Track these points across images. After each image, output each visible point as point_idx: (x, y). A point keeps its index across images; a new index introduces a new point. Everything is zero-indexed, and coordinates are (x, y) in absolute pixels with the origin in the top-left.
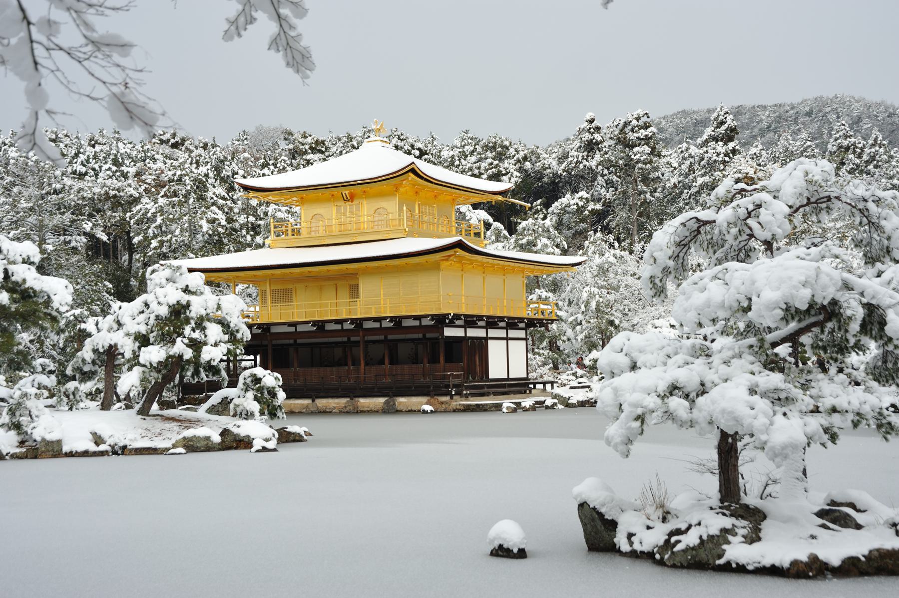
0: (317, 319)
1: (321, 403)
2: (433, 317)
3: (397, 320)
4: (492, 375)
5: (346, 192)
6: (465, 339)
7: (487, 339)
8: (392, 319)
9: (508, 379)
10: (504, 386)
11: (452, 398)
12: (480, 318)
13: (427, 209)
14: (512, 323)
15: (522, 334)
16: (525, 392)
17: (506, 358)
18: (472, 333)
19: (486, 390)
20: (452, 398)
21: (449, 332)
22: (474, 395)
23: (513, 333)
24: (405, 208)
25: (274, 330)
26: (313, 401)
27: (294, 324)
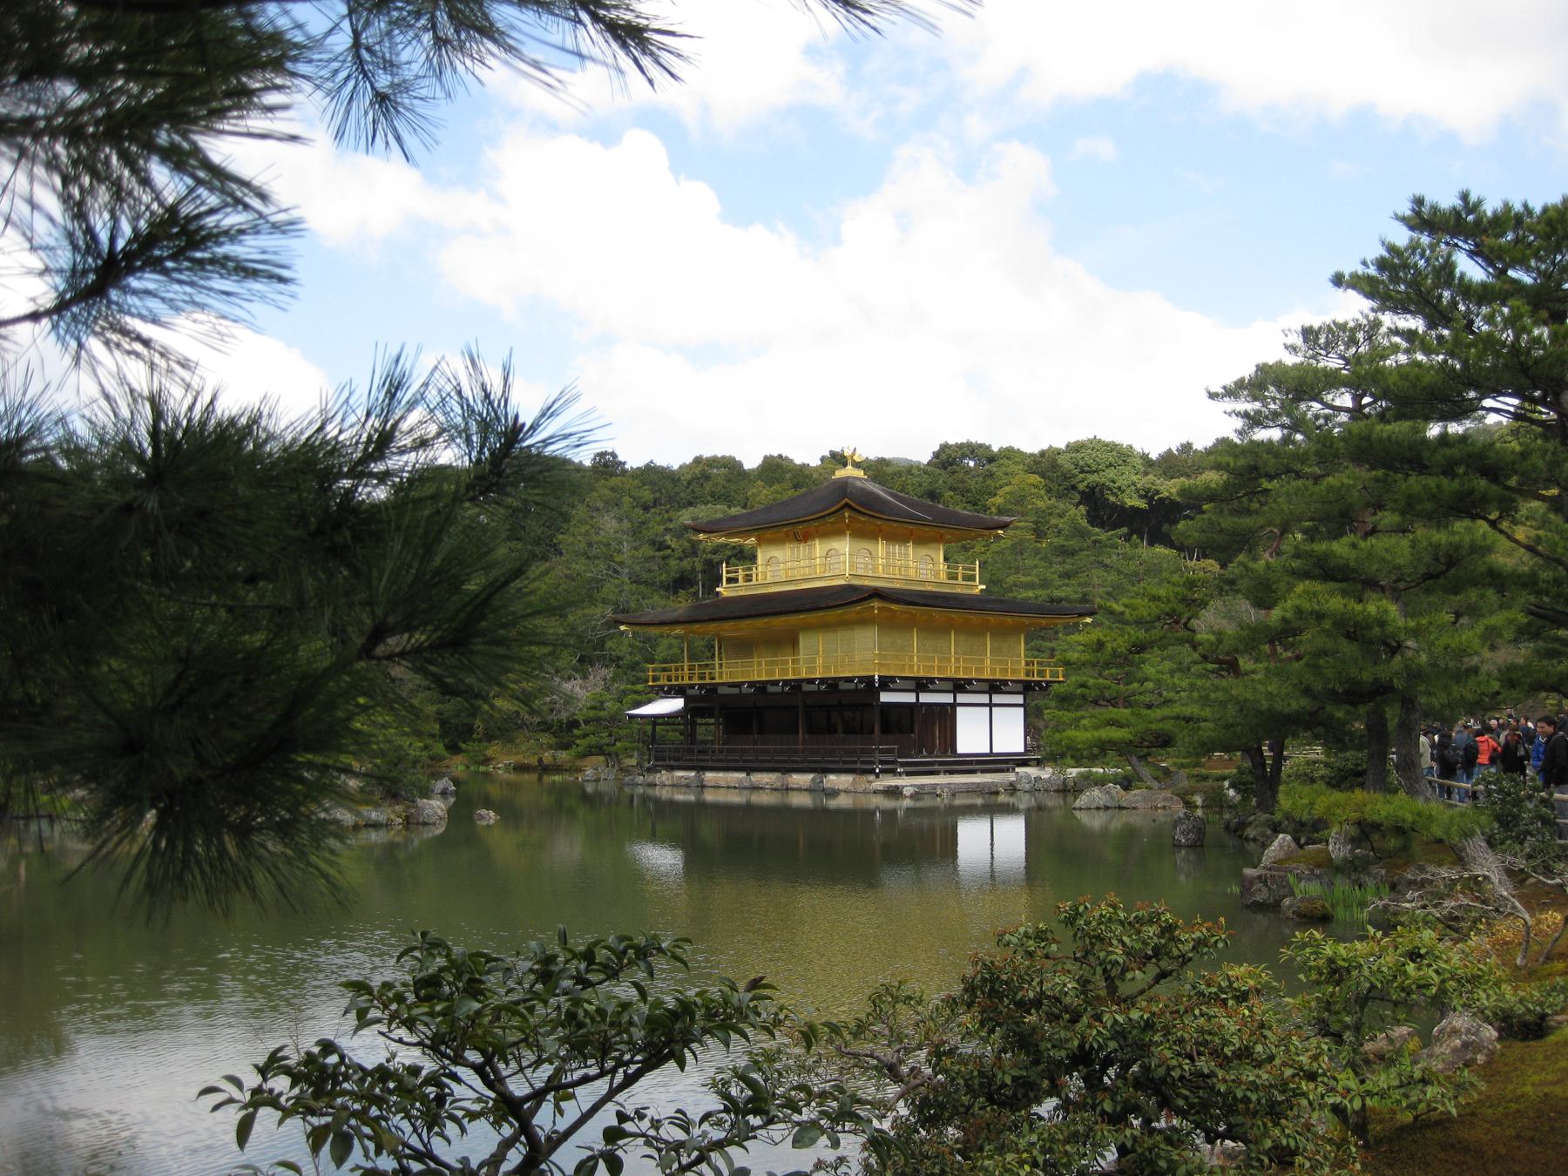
2: (861, 679)
3: (832, 684)
4: (961, 749)
6: (916, 706)
7: (954, 705)
8: (823, 681)
12: (932, 680)
13: (897, 549)
14: (994, 687)
15: (1019, 699)
18: (926, 698)
21: (886, 697)
22: (908, 774)
23: (997, 699)
25: (722, 690)
27: (739, 685)
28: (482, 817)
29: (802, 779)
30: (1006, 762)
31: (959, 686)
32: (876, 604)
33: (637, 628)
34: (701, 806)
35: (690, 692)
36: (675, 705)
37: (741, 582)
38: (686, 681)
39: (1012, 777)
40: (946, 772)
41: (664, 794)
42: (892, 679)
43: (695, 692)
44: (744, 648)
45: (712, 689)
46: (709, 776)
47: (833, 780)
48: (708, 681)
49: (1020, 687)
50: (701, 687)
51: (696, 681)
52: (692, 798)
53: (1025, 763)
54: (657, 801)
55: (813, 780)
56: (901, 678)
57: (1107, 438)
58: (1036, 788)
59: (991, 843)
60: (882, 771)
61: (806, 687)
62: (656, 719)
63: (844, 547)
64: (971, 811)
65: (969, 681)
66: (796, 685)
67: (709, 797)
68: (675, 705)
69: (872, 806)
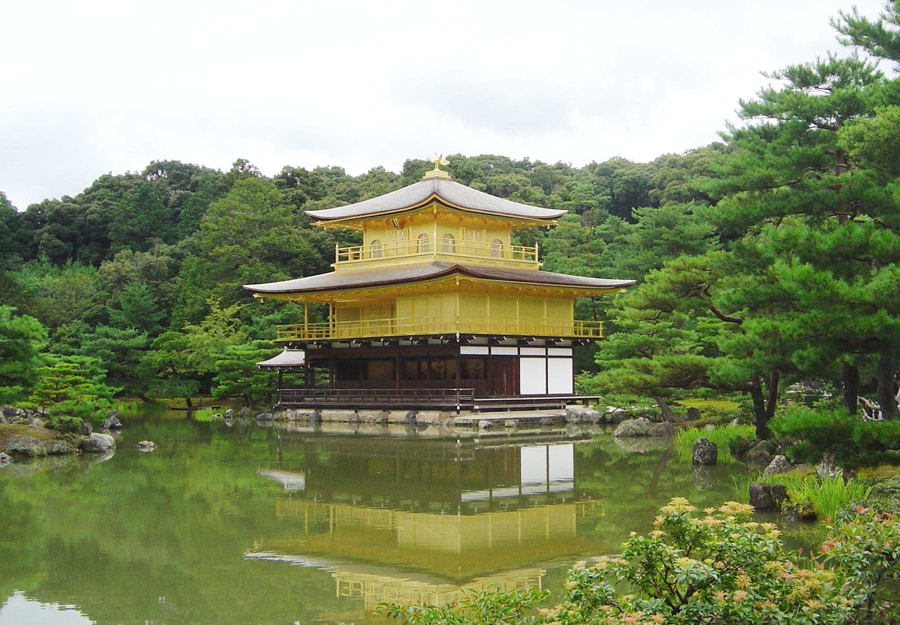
0: (358, 336)
1: (363, 414)
2: (446, 336)
3: (423, 340)
7: (518, 357)
8: (415, 337)
9: (547, 395)
10: (531, 402)
11: (458, 413)
12: (501, 337)
14: (550, 342)
15: (569, 352)
16: (560, 408)
17: (545, 375)
18: (496, 351)
19: (505, 406)
20: (458, 413)
21: (465, 350)
22: (483, 410)
23: (552, 351)
26: (356, 412)
27: (349, 341)
28: (143, 446)
29: (401, 415)
30: (559, 401)
31: (522, 341)
32: (458, 277)
34: (319, 434)
35: (309, 346)
36: (297, 357)
37: (350, 260)
38: (307, 339)
39: (563, 413)
40: (512, 409)
41: (290, 427)
42: (470, 336)
43: (314, 346)
44: (353, 313)
45: (328, 345)
46: (325, 413)
47: (424, 416)
48: (324, 338)
49: (569, 342)
50: (319, 342)
52: (312, 429)
53: (573, 402)
54: (284, 432)
55: (408, 416)
56: (477, 335)
58: (584, 421)
59: (547, 464)
60: (462, 409)
61: (403, 343)
62: (283, 368)
63: (434, 234)
64: (532, 440)
65: (530, 338)
66: (394, 341)
67: (325, 428)
68: (297, 357)
69: (454, 435)
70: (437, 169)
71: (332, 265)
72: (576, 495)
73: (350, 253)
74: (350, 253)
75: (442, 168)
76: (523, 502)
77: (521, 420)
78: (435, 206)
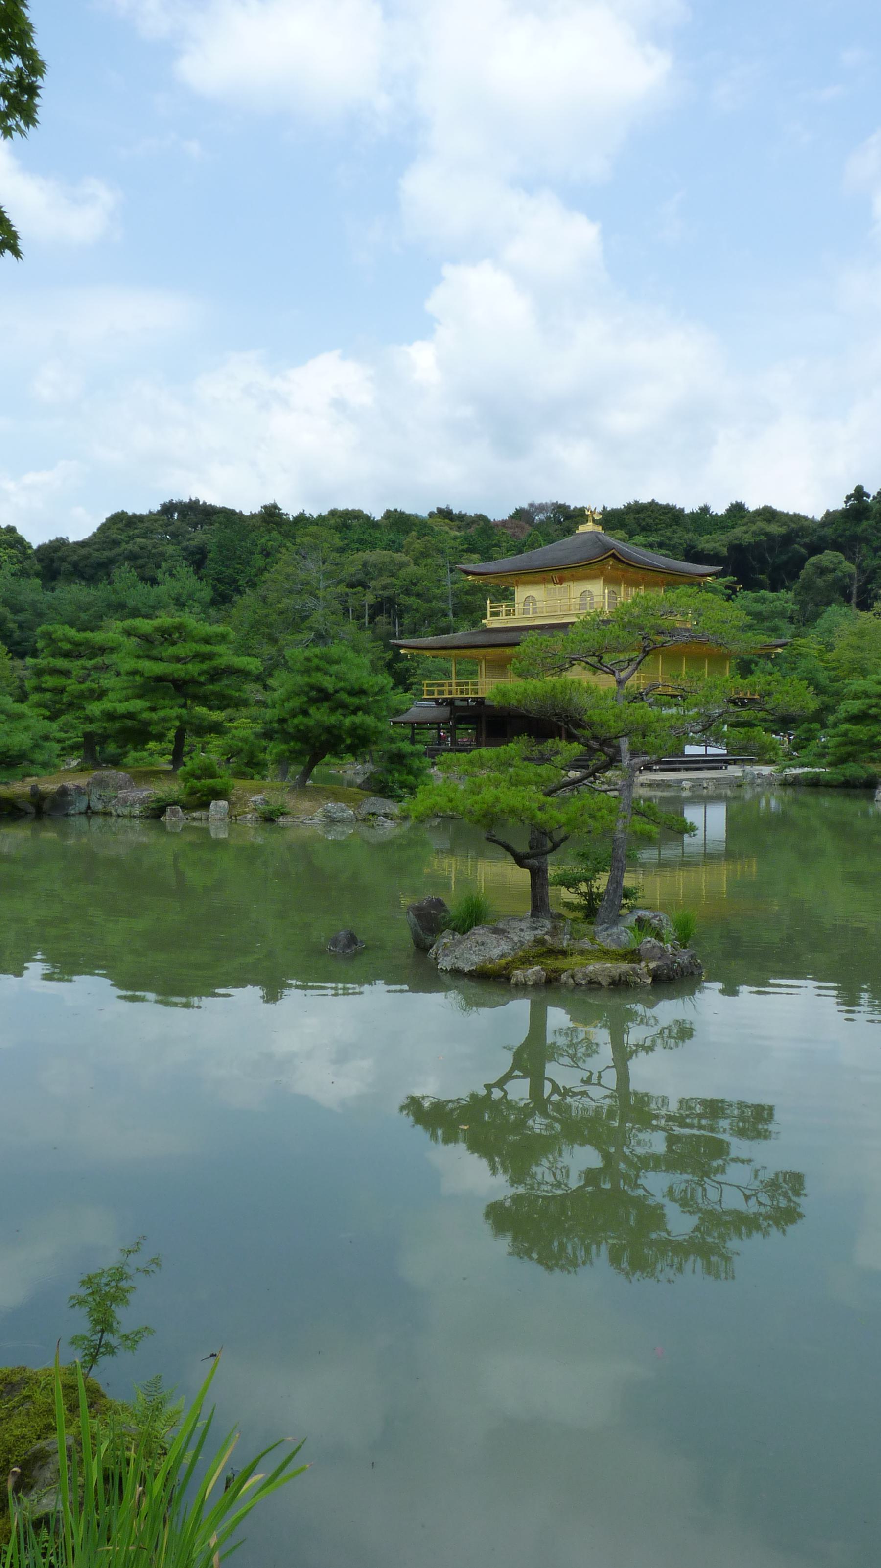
5: (556, 575)
16: (721, 768)
22: (663, 770)
24: (606, 591)
33: (415, 652)
35: (458, 703)
37: (503, 617)
40: (687, 769)
45: (480, 701)
48: (480, 695)
50: (474, 699)
51: (470, 696)
53: (727, 762)
57: (662, 501)
70: (590, 524)
71: (483, 621)
72: (729, 855)
73: (504, 609)
74: (504, 609)
75: (594, 521)
76: (686, 863)
77: (717, 779)
78: (611, 563)
